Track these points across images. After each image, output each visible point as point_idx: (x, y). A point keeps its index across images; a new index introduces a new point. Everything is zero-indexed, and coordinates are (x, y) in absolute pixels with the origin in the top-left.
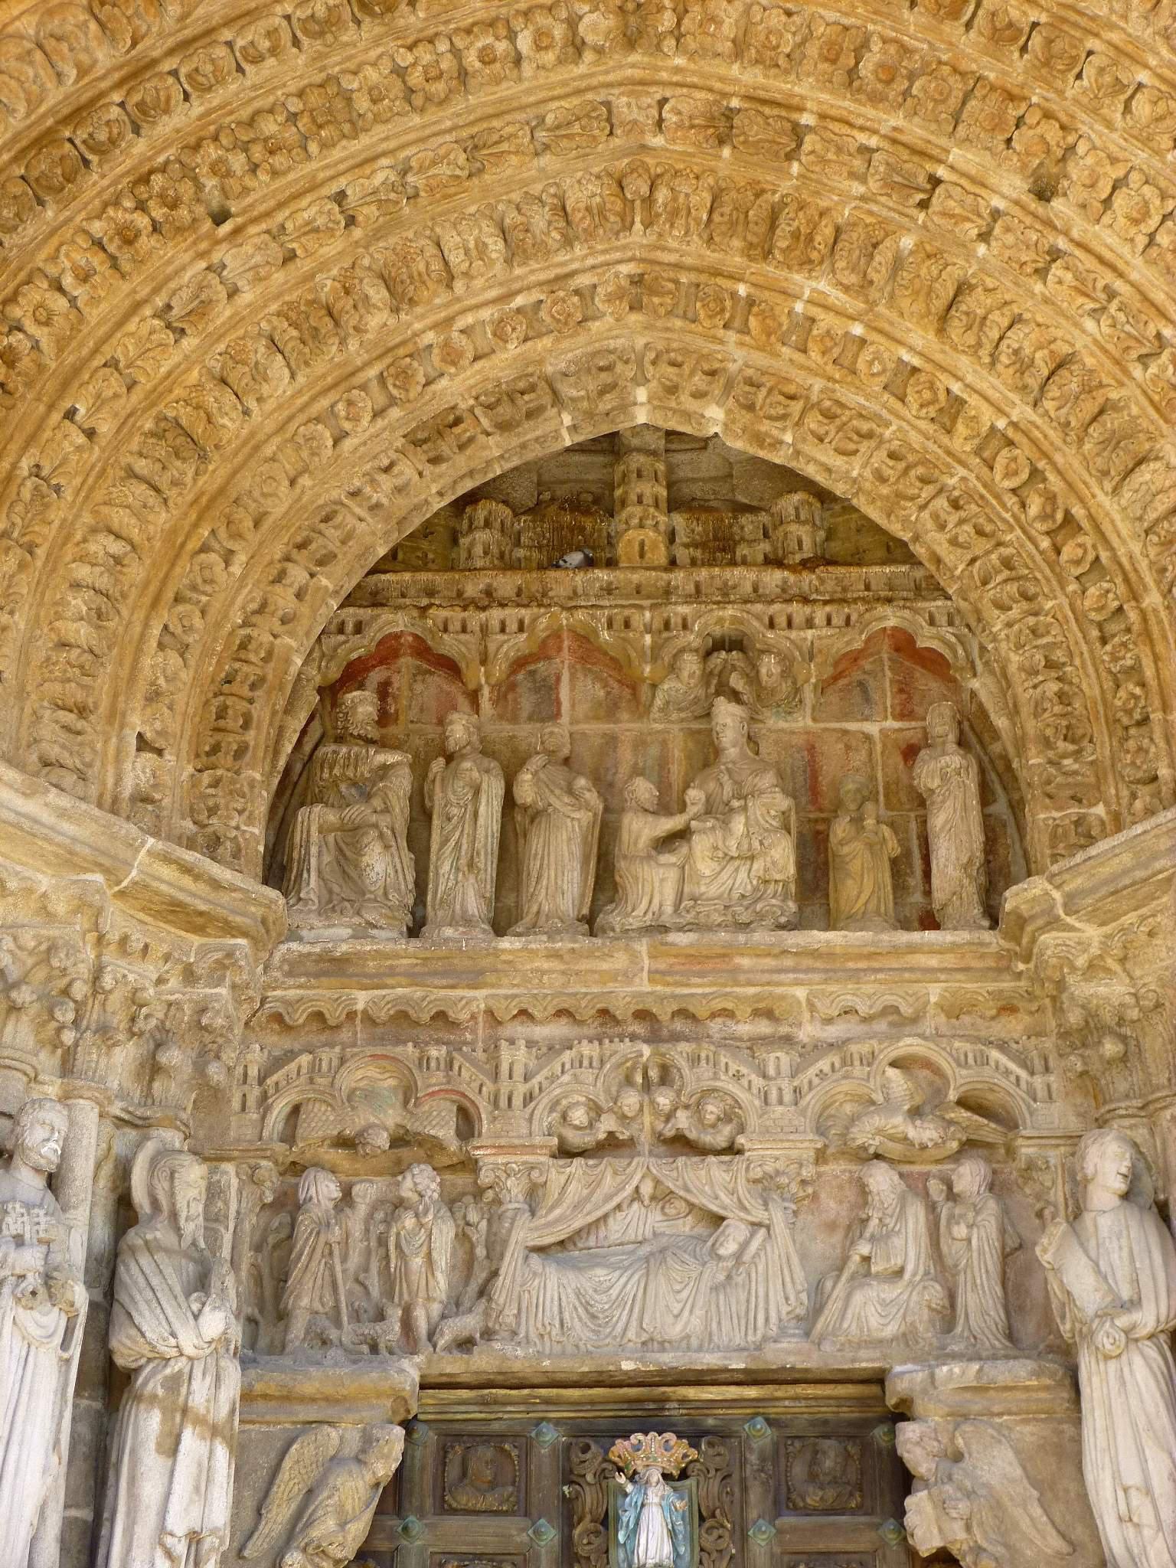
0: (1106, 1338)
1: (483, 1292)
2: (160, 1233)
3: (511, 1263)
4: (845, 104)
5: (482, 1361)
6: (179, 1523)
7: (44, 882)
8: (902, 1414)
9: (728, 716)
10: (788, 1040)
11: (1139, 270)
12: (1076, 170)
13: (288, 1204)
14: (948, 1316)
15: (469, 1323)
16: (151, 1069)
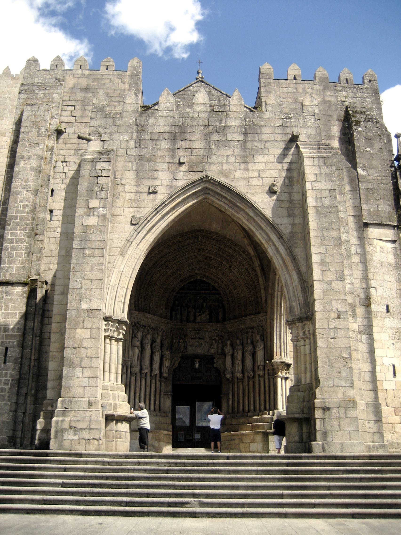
0: (228, 354)
1: (186, 349)
2: (165, 346)
3: (188, 347)
4: (215, 258)
5: (186, 354)
6: (167, 365)
7: (157, 322)
8: (214, 358)
9: (205, 304)
10: (208, 331)
11: (237, 275)
12: (233, 266)
13: (172, 342)
14: (218, 351)
15: (185, 351)
16: (163, 333)
